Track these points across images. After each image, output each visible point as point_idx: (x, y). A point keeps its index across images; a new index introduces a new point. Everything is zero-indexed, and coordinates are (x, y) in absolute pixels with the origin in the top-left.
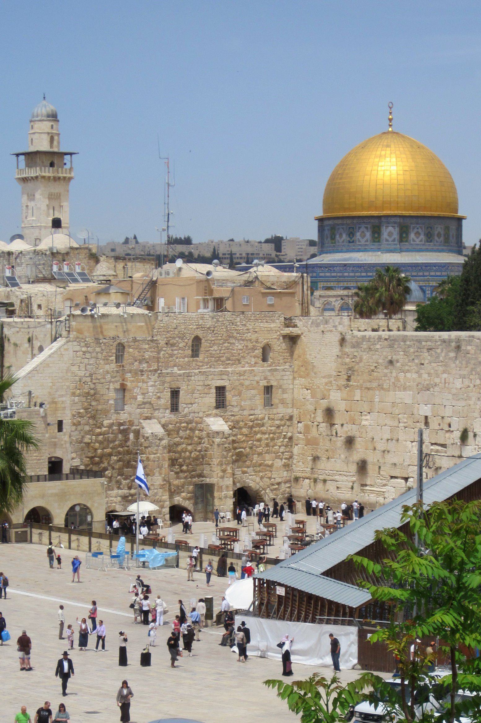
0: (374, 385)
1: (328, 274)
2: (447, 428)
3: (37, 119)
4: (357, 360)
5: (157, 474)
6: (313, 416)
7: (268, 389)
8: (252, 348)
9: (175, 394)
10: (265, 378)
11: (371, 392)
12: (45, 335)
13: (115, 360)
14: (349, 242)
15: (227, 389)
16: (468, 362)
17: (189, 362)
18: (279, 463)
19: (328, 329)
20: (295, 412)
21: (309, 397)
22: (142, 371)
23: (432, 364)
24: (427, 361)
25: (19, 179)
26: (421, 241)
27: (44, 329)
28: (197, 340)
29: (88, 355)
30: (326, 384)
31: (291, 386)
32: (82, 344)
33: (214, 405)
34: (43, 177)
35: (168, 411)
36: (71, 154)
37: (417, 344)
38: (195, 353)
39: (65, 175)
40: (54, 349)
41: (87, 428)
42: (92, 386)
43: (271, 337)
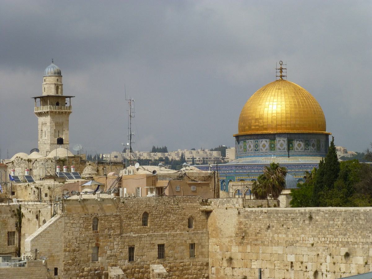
1: (241, 171)
3: (48, 75)
4: (248, 226)
6: (221, 262)
7: (192, 246)
8: (182, 219)
9: (131, 249)
10: (190, 238)
11: (257, 246)
12: (47, 213)
13: (92, 229)
14: (255, 150)
15: (165, 246)
16: (317, 227)
17: (140, 228)
19: (229, 206)
20: (210, 261)
21: (218, 250)
22: (110, 235)
24: (291, 227)
25: (36, 113)
26: (302, 149)
27: (46, 209)
28: (146, 215)
30: (229, 242)
33: (157, 256)
34: (52, 112)
35: (127, 261)
36: (70, 97)
37: (285, 215)
38: (145, 223)
39: (66, 111)
40: (52, 222)
41: (73, 272)
42: (77, 245)
43: (193, 212)
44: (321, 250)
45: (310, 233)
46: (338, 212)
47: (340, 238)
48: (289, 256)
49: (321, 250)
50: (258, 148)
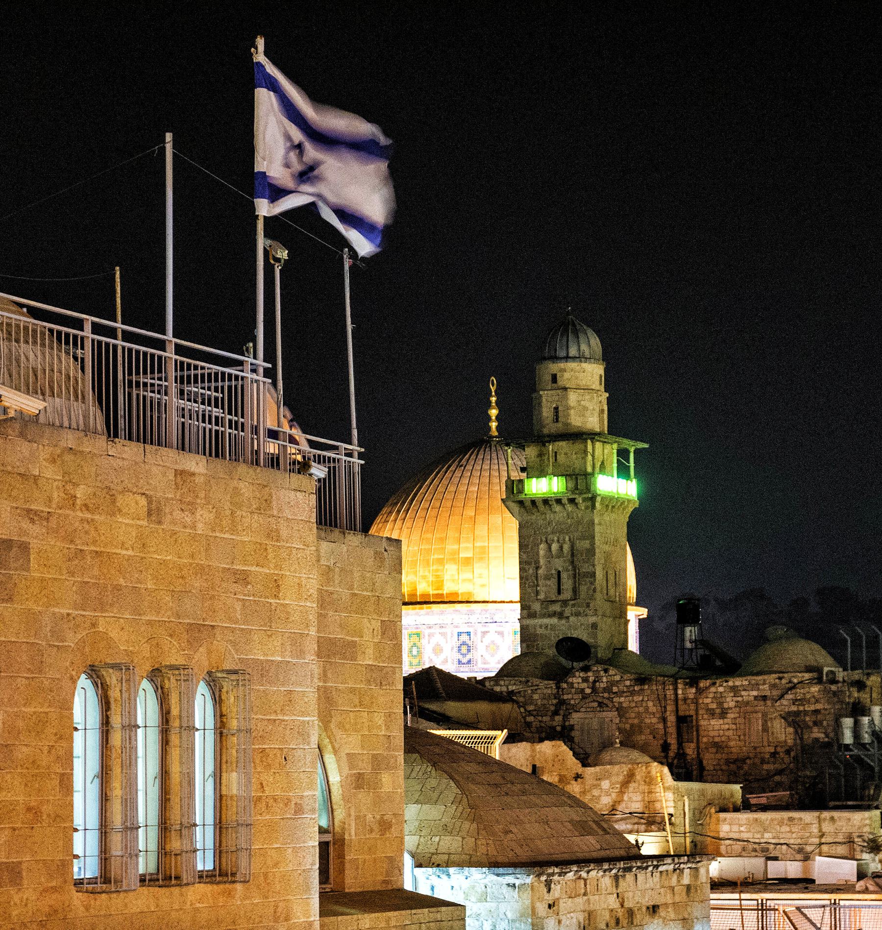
50: (468, 657)
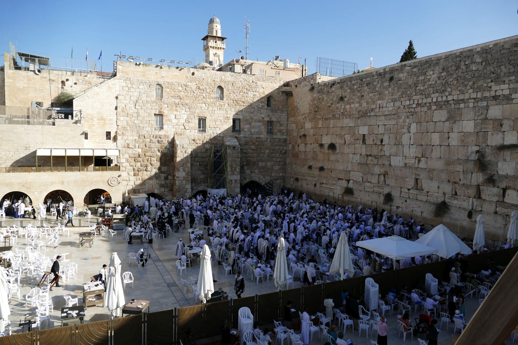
0: (330, 116)
2: (380, 144)
5: (181, 170)
10: (268, 116)
18: (277, 168)
21: (295, 128)
23: (371, 95)
24: (366, 93)
29: (132, 90)
31: (286, 123)
32: (128, 82)
34: (211, 47)
37: (359, 81)
41: (131, 138)
44: (403, 117)
45: (390, 97)
46: (434, 62)
47: (435, 97)
48: (361, 128)
49: (403, 117)
